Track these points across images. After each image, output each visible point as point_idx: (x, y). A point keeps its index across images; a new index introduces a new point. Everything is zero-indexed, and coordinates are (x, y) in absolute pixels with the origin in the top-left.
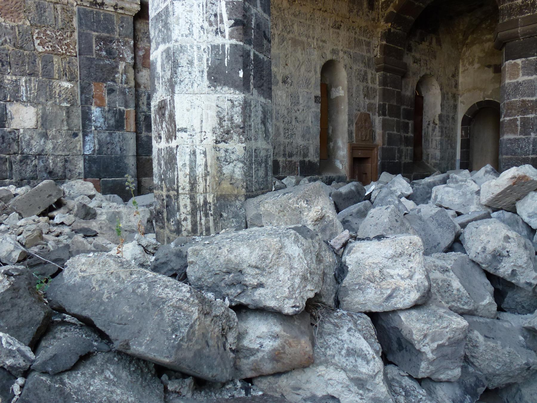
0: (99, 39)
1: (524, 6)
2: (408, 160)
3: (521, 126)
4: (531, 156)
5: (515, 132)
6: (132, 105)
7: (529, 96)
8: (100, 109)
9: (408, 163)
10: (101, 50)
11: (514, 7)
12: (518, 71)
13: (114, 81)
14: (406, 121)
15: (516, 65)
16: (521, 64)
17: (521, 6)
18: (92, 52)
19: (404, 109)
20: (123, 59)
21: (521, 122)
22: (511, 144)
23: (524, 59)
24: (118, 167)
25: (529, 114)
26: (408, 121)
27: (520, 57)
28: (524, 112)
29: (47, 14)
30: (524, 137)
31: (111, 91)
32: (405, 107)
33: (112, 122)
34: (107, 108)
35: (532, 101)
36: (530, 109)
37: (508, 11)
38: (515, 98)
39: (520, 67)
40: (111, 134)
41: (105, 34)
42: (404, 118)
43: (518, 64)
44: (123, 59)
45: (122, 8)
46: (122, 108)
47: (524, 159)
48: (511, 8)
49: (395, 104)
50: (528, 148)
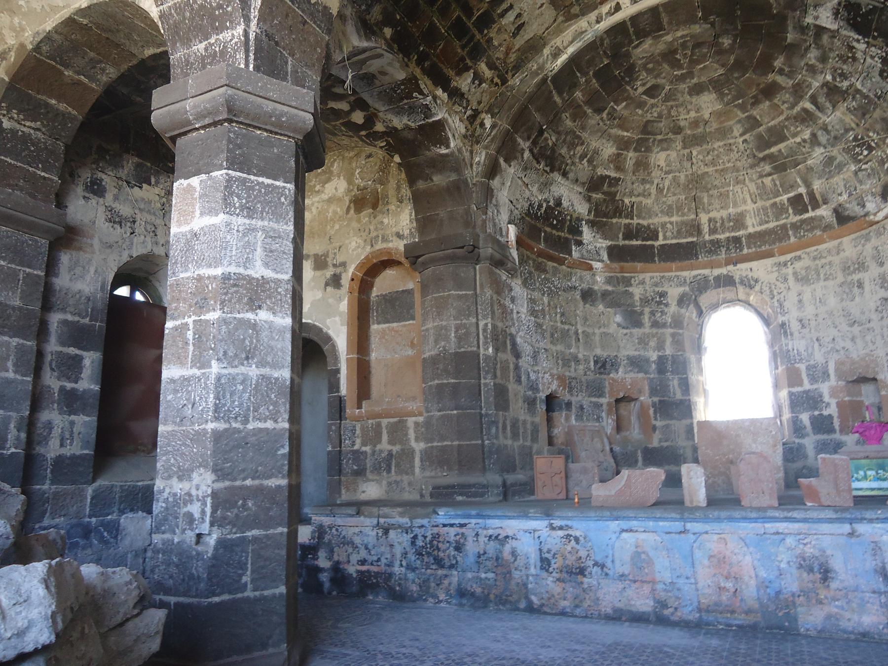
1: (208, 57)
2: (75, 449)
3: (194, 345)
4: (211, 426)
5: (180, 361)
7: (210, 266)
9: (73, 457)
11: (192, 60)
12: (193, 206)
14: (72, 351)
15: (190, 189)
16: (198, 189)
17: (203, 58)
19: (65, 322)
21: (195, 334)
22: (176, 391)
23: (203, 177)
25: (208, 311)
26: (78, 352)
27: (197, 173)
28: (201, 307)
30: (197, 372)
32: (69, 317)
35: (215, 277)
36: (211, 298)
37: (182, 70)
38: (186, 271)
39: (197, 195)
42: (63, 344)
43: (194, 189)
47: (197, 433)
48: (187, 61)
49: (17, 303)
50: (206, 402)
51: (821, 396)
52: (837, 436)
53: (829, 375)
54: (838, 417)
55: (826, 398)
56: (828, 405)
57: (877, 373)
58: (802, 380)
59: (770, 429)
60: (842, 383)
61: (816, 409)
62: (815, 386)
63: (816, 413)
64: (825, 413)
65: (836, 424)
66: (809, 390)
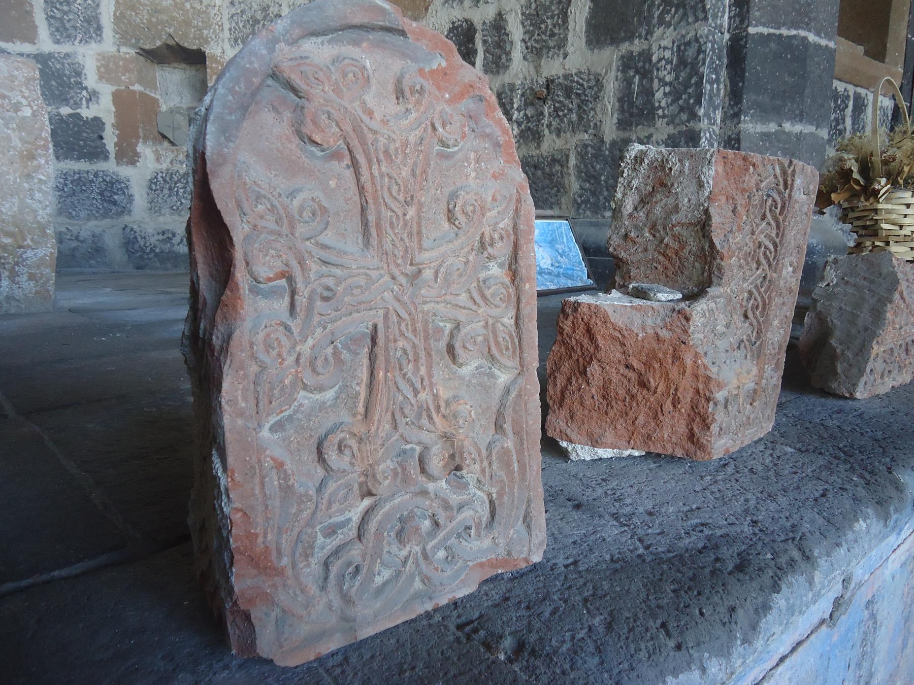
51: (78, 74)
52: (110, 166)
53: (99, 28)
54: (116, 126)
55: (91, 80)
56: (93, 96)
57: (207, 42)
58: (35, 28)
59: (16, 97)
60: (128, 51)
61: (66, 101)
62: (65, 48)
63: (65, 111)
64: (87, 113)
65: (110, 139)
66: (51, 56)
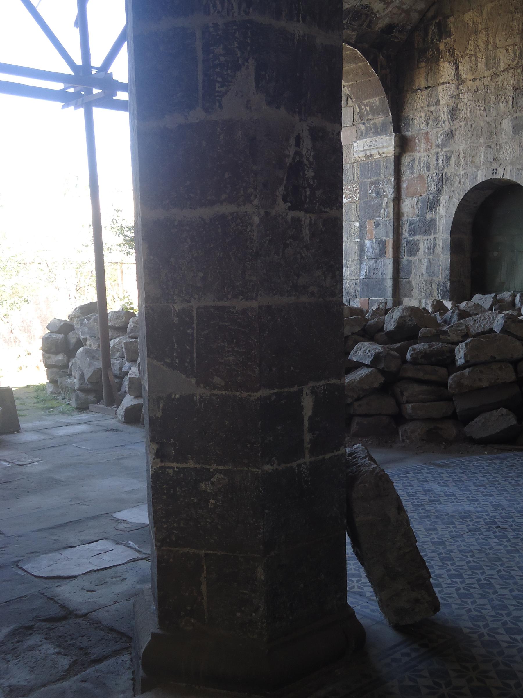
0: (372, 183)
6: (391, 234)
8: (370, 242)
10: (372, 193)
13: (379, 216)
18: (367, 196)
20: (386, 196)
24: (380, 289)
29: (349, 173)
31: (378, 225)
33: (377, 251)
34: (374, 240)
40: (376, 261)
41: (374, 179)
44: (386, 196)
45: (383, 153)
46: (384, 238)
